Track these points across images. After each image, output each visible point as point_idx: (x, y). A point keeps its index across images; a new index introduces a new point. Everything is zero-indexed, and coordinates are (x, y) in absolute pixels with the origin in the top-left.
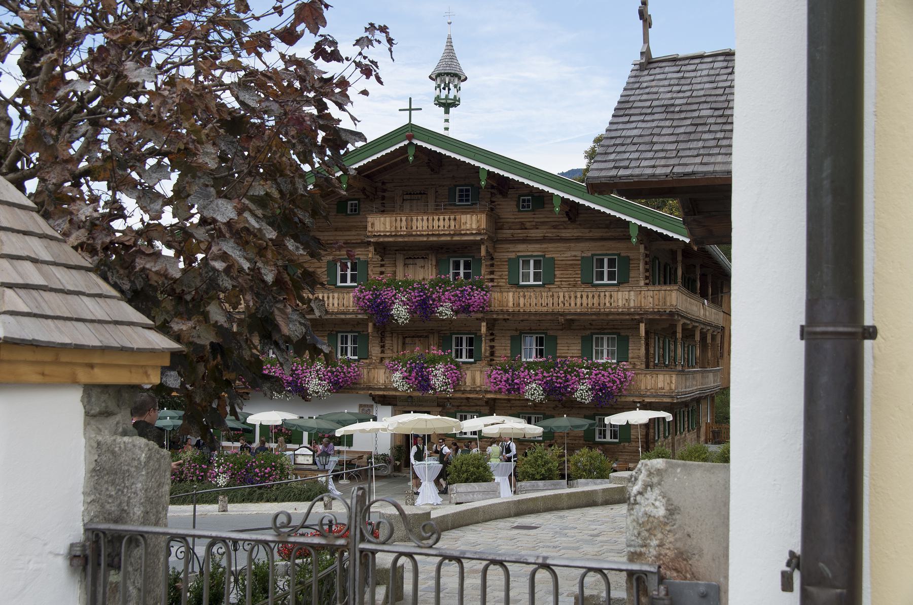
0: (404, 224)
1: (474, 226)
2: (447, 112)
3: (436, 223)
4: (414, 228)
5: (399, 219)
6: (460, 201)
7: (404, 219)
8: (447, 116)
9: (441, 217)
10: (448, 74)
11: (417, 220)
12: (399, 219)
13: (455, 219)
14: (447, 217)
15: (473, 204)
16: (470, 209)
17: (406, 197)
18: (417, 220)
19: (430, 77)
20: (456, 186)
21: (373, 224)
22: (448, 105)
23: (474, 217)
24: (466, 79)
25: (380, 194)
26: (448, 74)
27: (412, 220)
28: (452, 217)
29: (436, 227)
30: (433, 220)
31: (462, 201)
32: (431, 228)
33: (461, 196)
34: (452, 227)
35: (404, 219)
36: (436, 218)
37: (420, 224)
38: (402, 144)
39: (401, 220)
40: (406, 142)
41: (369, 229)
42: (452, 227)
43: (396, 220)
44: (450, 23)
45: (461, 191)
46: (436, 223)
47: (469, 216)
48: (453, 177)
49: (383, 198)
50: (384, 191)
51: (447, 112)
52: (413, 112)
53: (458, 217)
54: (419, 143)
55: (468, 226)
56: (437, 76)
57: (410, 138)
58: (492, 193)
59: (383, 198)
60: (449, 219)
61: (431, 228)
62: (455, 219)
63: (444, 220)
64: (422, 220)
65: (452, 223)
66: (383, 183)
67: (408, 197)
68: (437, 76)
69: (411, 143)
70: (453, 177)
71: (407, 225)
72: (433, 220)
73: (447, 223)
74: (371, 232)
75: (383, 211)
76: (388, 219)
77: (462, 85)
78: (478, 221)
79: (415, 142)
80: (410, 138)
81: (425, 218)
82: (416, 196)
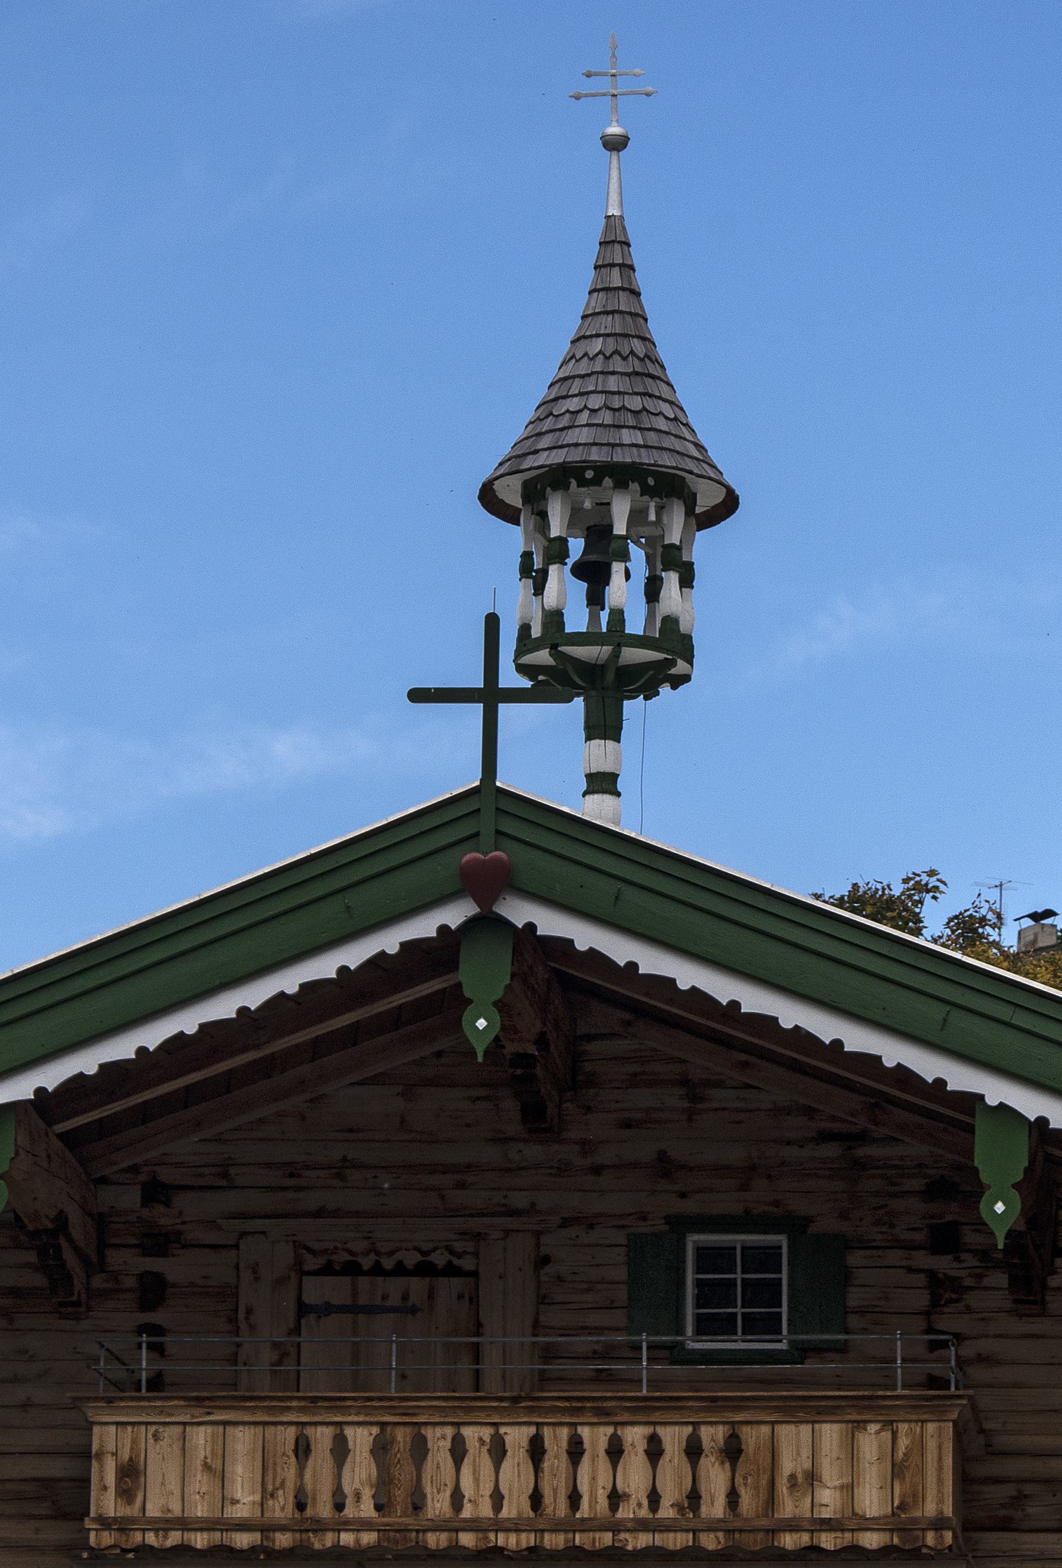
0: (360, 1471)
1: (872, 1501)
2: (604, 726)
3: (594, 1478)
4: (438, 1505)
5: (322, 1437)
6: (705, 1326)
7: (361, 1438)
8: (600, 755)
9: (635, 1436)
10: (623, 475)
11: (458, 1451)
12: (322, 1437)
13: (732, 1452)
14: (673, 1438)
15: (801, 1352)
16: (826, 1381)
17: (321, 1290)
18: (458, 1451)
19: (488, 497)
20: (681, 1224)
21: (131, 1474)
22: (608, 679)
23: (871, 1442)
24: (730, 504)
25: (130, 1262)
26: (623, 475)
27: (420, 1449)
28: (712, 1435)
29: (594, 1504)
30: (576, 1451)
31: (724, 1326)
32: (556, 1505)
33: (706, 1294)
34: (715, 1508)
35: (361, 1438)
36: (595, 1437)
37: (476, 1480)
38: (423, 927)
39: (341, 1450)
40: (454, 915)
41: (106, 1501)
42: (715, 1508)
43: (303, 1449)
44: (616, 145)
45: (707, 1258)
46: (594, 1478)
47: (830, 1433)
48: (665, 1166)
49: (153, 1291)
50: (159, 1242)
51: (604, 726)
52: (506, 711)
53: (753, 1437)
54: (552, 924)
55: (829, 1500)
56: (520, 492)
57: (486, 884)
58: (935, 1281)
59: (153, 1291)
60: (693, 1451)
61: (556, 1505)
62: (732, 1452)
63: (654, 1451)
64: (498, 1451)
65: (715, 1478)
66: (156, 1192)
67: (334, 1289)
68: (520, 492)
69: (487, 923)
70: (665, 1166)
71: (384, 1486)
72: (576, 1451)
73: (635, 1475)
74: (122, 1525)
75: (156, 1383)
76: (243, 1440)
77: (705, 548)
78: (898, 1470)
79: (519, 912)
80: (486, 884)
81: (517, 1437)
82: (394, 1287)
